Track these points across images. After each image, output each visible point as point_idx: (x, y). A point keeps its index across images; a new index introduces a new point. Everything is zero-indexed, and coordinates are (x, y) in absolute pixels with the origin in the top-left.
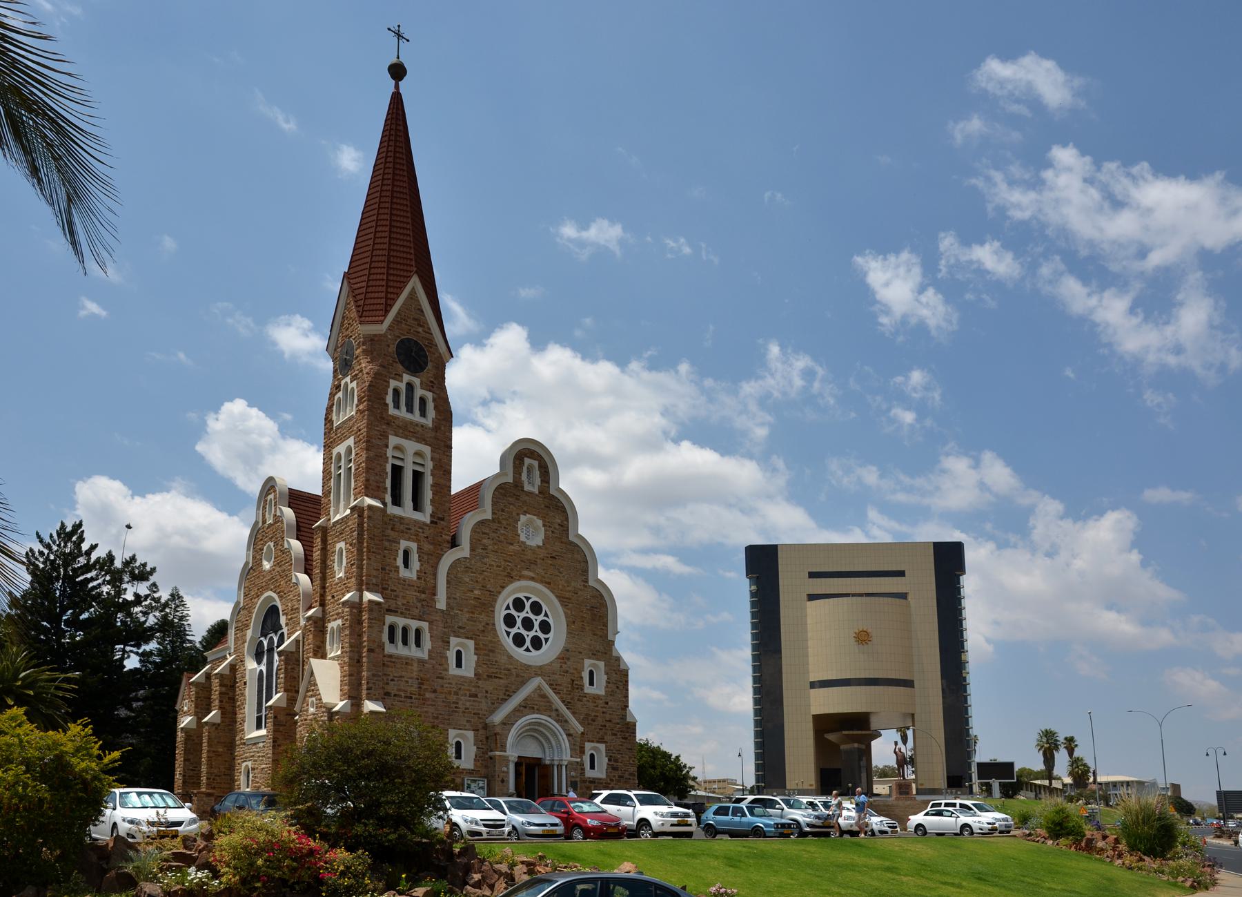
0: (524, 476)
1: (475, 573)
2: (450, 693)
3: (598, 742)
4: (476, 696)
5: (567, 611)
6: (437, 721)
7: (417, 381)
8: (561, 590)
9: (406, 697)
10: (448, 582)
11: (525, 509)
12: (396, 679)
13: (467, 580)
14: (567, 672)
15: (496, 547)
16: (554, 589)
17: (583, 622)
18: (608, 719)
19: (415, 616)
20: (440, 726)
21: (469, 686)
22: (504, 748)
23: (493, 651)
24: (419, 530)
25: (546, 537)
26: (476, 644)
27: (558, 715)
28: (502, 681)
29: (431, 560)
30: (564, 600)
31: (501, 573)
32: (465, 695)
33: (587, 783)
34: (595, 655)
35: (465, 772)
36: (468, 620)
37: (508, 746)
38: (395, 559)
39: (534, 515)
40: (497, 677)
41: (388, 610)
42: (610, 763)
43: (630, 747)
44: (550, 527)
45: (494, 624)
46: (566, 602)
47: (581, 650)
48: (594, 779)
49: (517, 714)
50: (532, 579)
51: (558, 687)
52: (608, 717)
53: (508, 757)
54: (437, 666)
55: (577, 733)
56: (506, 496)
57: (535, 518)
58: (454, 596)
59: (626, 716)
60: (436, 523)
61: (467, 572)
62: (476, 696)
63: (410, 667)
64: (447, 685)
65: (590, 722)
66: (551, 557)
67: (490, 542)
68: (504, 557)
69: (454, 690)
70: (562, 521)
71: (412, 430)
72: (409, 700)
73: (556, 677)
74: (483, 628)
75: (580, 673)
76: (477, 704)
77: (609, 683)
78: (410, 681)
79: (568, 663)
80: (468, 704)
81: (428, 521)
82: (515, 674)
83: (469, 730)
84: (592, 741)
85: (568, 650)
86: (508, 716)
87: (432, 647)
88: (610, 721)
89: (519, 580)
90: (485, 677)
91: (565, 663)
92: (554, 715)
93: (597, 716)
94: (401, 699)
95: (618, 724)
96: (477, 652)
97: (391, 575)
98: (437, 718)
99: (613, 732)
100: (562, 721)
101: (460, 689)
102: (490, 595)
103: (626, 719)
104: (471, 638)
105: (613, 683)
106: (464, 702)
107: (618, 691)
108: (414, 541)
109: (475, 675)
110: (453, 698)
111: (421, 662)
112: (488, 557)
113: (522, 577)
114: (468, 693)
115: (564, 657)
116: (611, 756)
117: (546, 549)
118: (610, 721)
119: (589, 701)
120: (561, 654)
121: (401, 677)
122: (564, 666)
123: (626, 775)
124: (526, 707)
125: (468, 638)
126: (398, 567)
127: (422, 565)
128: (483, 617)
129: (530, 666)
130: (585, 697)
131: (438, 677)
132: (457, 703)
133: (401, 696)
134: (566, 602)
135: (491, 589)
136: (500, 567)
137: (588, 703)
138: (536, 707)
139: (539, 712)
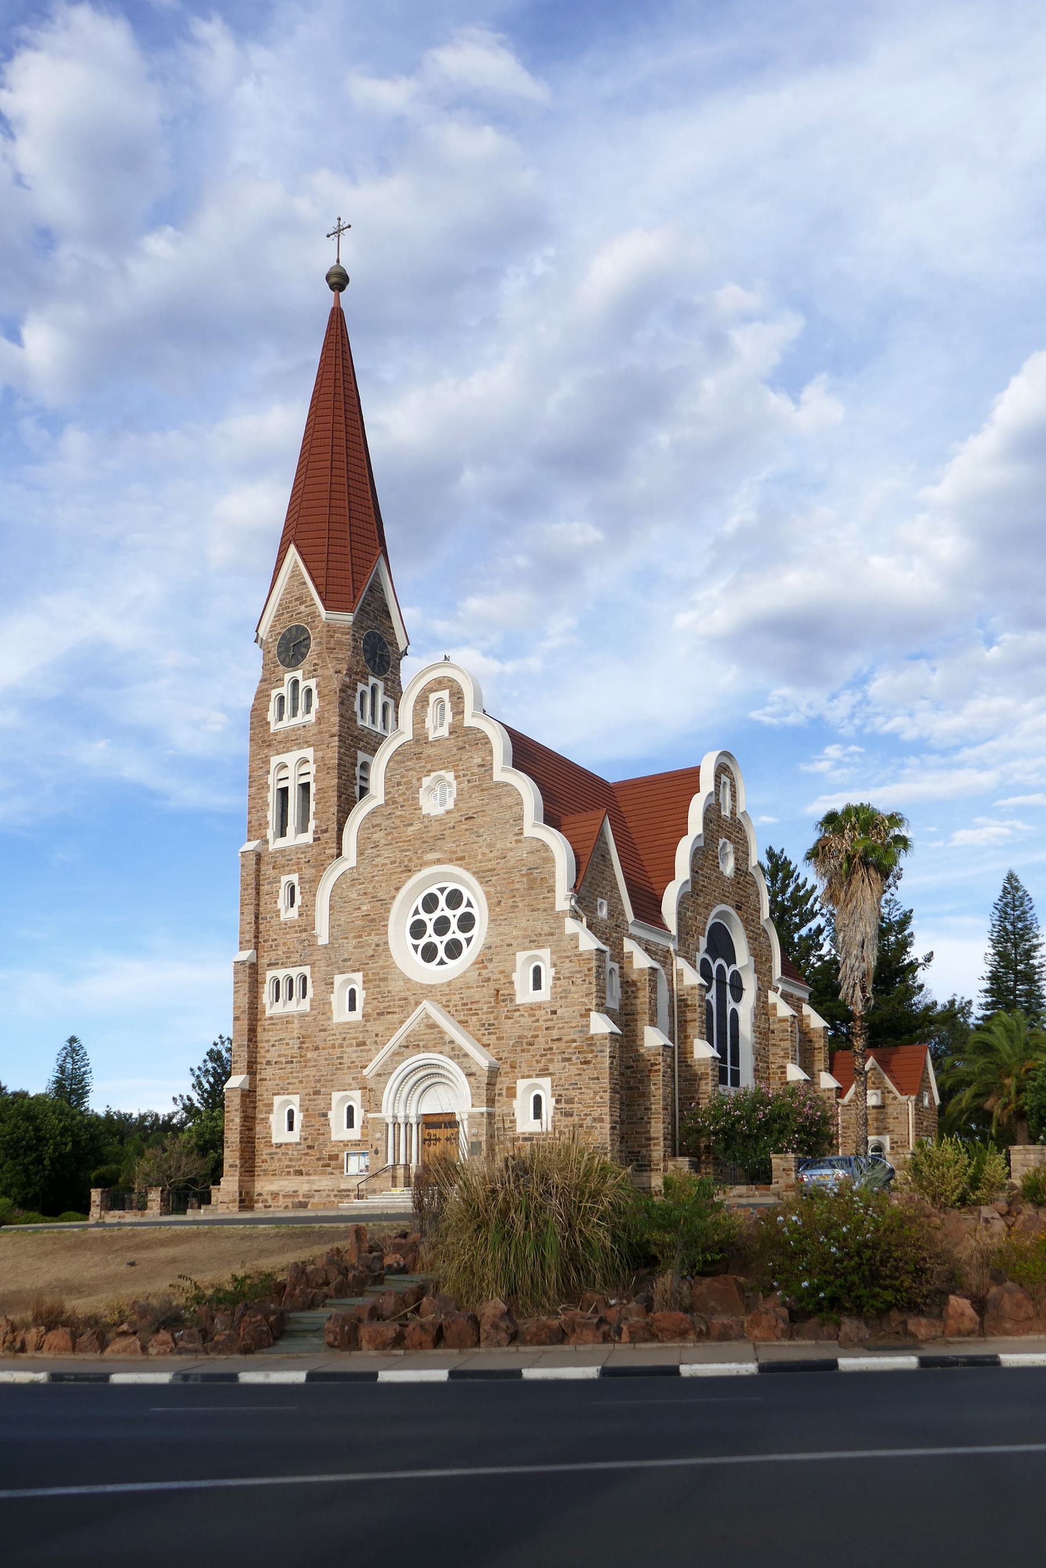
0: (429, 723)
1: (363, 883)
2: (333, 1046)
3: (538, 1076)
4: (364, 1043)
5: (488, 889)
6: (318, 1085)
7: (298, 674)
8: (480, 862)
9: (287, 1062)
10: (331, 907)
11: (429, 766)
12: (277, 1043)
13: (354, 896)
14: (488, 980)
15: (389, 838)
16: (469, 864)
17: (514, 896)
18: (555, 1038)
19: (296, 962)
20: (322, 1090)
21: (356, 1032)
22: (378, 1108)
23: (384, 979)
24: (300, 856)
25: (460, 793)
26: (364, 976)
27: (453, 1049)
28: (396, 1016)
29: (311, 884)
30: (482, 876)
31: (396, 870)
32: (351, 1045)
33: (520, 1142)
34: (534, 941)
35: (350, 1144)
36: (354, 948)
37: (384, 1104)
38: (276, 902)
39: (441, 769)
40: (389, 1013)
41: (269, 965)
42: (560, 1107)
43: (596, 1076)
44: (464, 776)
45: (386, 943)
46: (487, 876)
47: (511, 941)
48: (530, 1134)
49: (396, 1058)
50: (438, 861)
51: (474, 1006)
52: (555, 1034)
53: (384, 1119)
54: (320, 1017)
55: (482, 1069)
56: (403, 762)
57: (442, 773)
58: (338, 923)
59: (588, 1026)
60: (319, 839)
61: (353, 885)
62: (364, 1043)
63: (290, 1025)
64: (329, 1038)
65: (525, 1047)
66: (466, 819)
67: (382, 834)
68: (399, 847)
69: (339, 1041)
70: (483, 760)
71: (293, 738)
72: (289, 1066)
73: (472, 990)
74: (372, 953)
75: (509, 976)
76: (365, 1054)
77: (559, 979)
78: (291, 1042)
79: (490, 966)
80: (354, 1055)
81: (311, 841)
82: (413, 1002)
83: (355, 1089)
84: (529, 1077)
85: (489, 948)
86: (385, 1064)
87: (314, 995)
88: (559, 1039)
89: (420, 870)
90: (376, 1016)
91: (486, 967)
92: (447, 1049)
93: (537, 1036)
94: (281, 1066)
95: (574, 1041)
96: (366, 986)
97: (273, 922)
98: (319, 1081)
99: (566, 1056)
100: (459, 1055)
101: (344, 1039)
102: (382, 905)
103: (589, 1031)
104: (359, 970)
105: (565, 978)
106: (351, 1054)
107: (573, 988)
108: (295, 872)
109: (363, 1016)
110: (337, 1052)
111: (303, 1016)
112: (379, 856)
113: (424, 864)
114: (354, 1042)
115: (481, 962)
116: (560, 1095)
117: (458, 810)
118: (559, 1039)
119: (523, 1016)
120: (479, 955)
121: (281, 1040)
122: (484, 972)
123: (588, 1121)
124: (410, 1046)
125: (354, 971)
126: (279, 911)
127: (303, 898)
128: (374, 939)
129: (433, 986)
130: (518, 1010)
131: (321, 1030)
132: (342, 1057)
133: (281, 1063)
134: (487, 876)
135: (383, 897)
136: (395, 862)
137: (522, 1020)
138: (421, 1044)
139: (426, 1048)
